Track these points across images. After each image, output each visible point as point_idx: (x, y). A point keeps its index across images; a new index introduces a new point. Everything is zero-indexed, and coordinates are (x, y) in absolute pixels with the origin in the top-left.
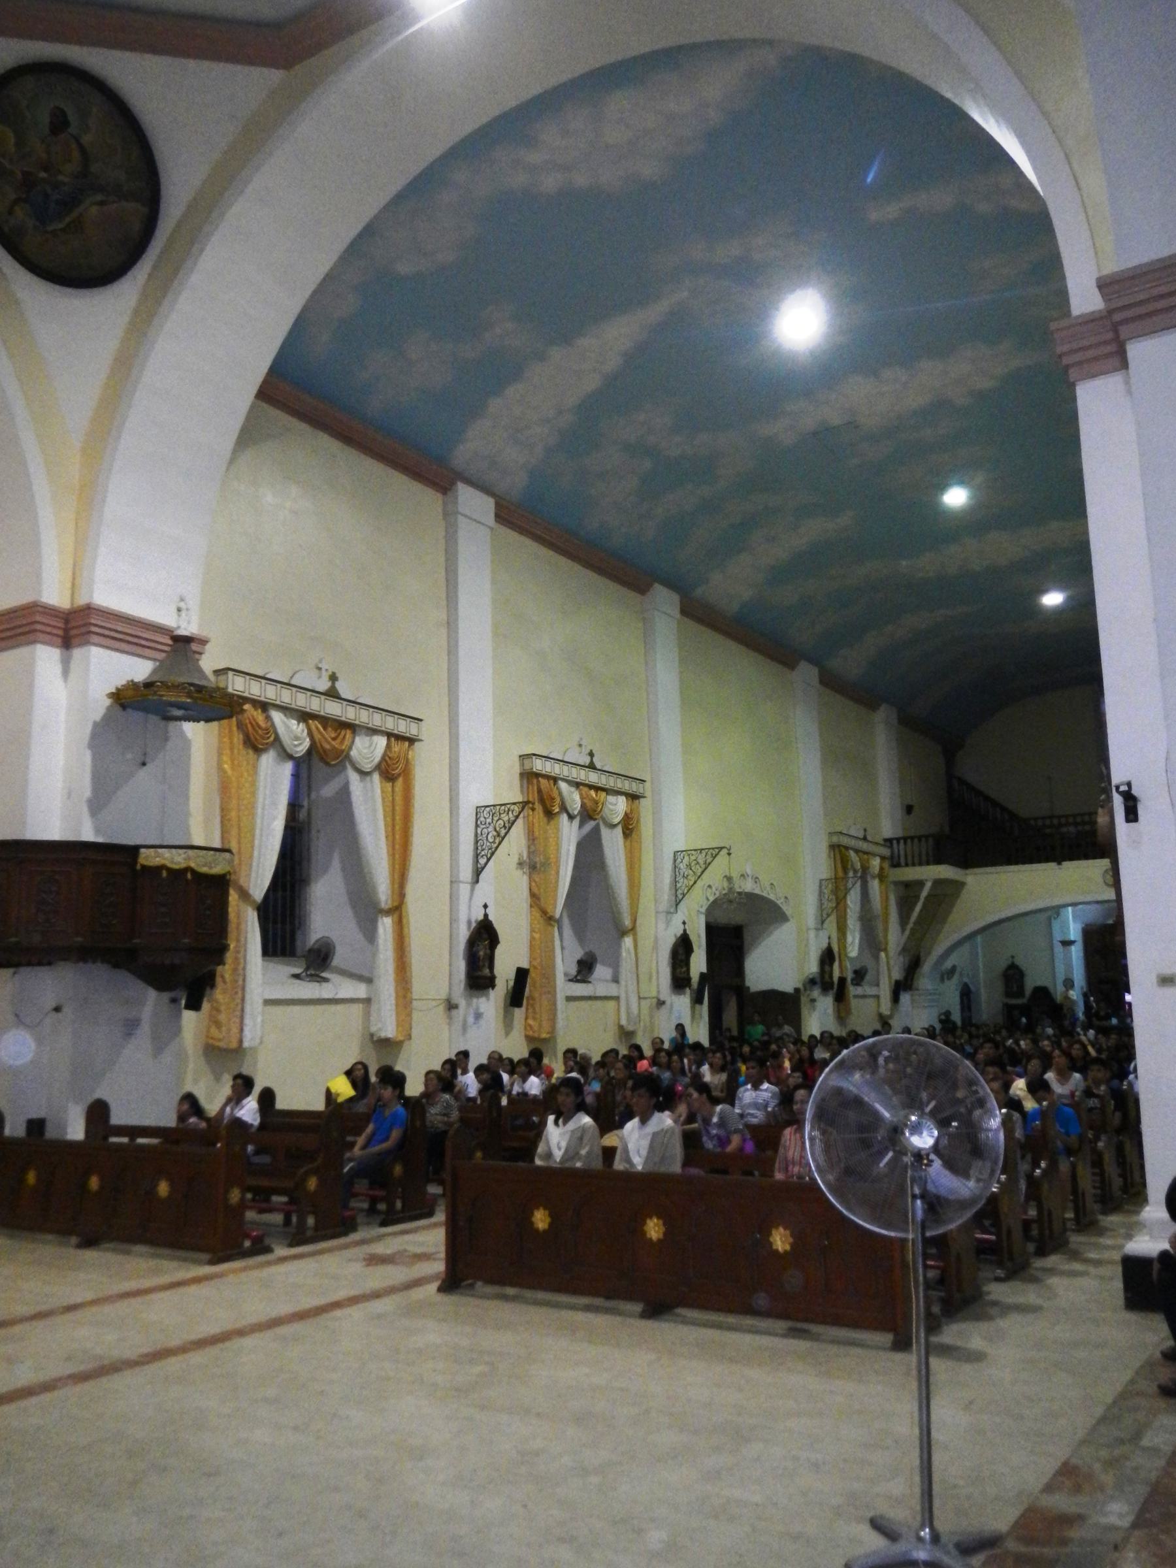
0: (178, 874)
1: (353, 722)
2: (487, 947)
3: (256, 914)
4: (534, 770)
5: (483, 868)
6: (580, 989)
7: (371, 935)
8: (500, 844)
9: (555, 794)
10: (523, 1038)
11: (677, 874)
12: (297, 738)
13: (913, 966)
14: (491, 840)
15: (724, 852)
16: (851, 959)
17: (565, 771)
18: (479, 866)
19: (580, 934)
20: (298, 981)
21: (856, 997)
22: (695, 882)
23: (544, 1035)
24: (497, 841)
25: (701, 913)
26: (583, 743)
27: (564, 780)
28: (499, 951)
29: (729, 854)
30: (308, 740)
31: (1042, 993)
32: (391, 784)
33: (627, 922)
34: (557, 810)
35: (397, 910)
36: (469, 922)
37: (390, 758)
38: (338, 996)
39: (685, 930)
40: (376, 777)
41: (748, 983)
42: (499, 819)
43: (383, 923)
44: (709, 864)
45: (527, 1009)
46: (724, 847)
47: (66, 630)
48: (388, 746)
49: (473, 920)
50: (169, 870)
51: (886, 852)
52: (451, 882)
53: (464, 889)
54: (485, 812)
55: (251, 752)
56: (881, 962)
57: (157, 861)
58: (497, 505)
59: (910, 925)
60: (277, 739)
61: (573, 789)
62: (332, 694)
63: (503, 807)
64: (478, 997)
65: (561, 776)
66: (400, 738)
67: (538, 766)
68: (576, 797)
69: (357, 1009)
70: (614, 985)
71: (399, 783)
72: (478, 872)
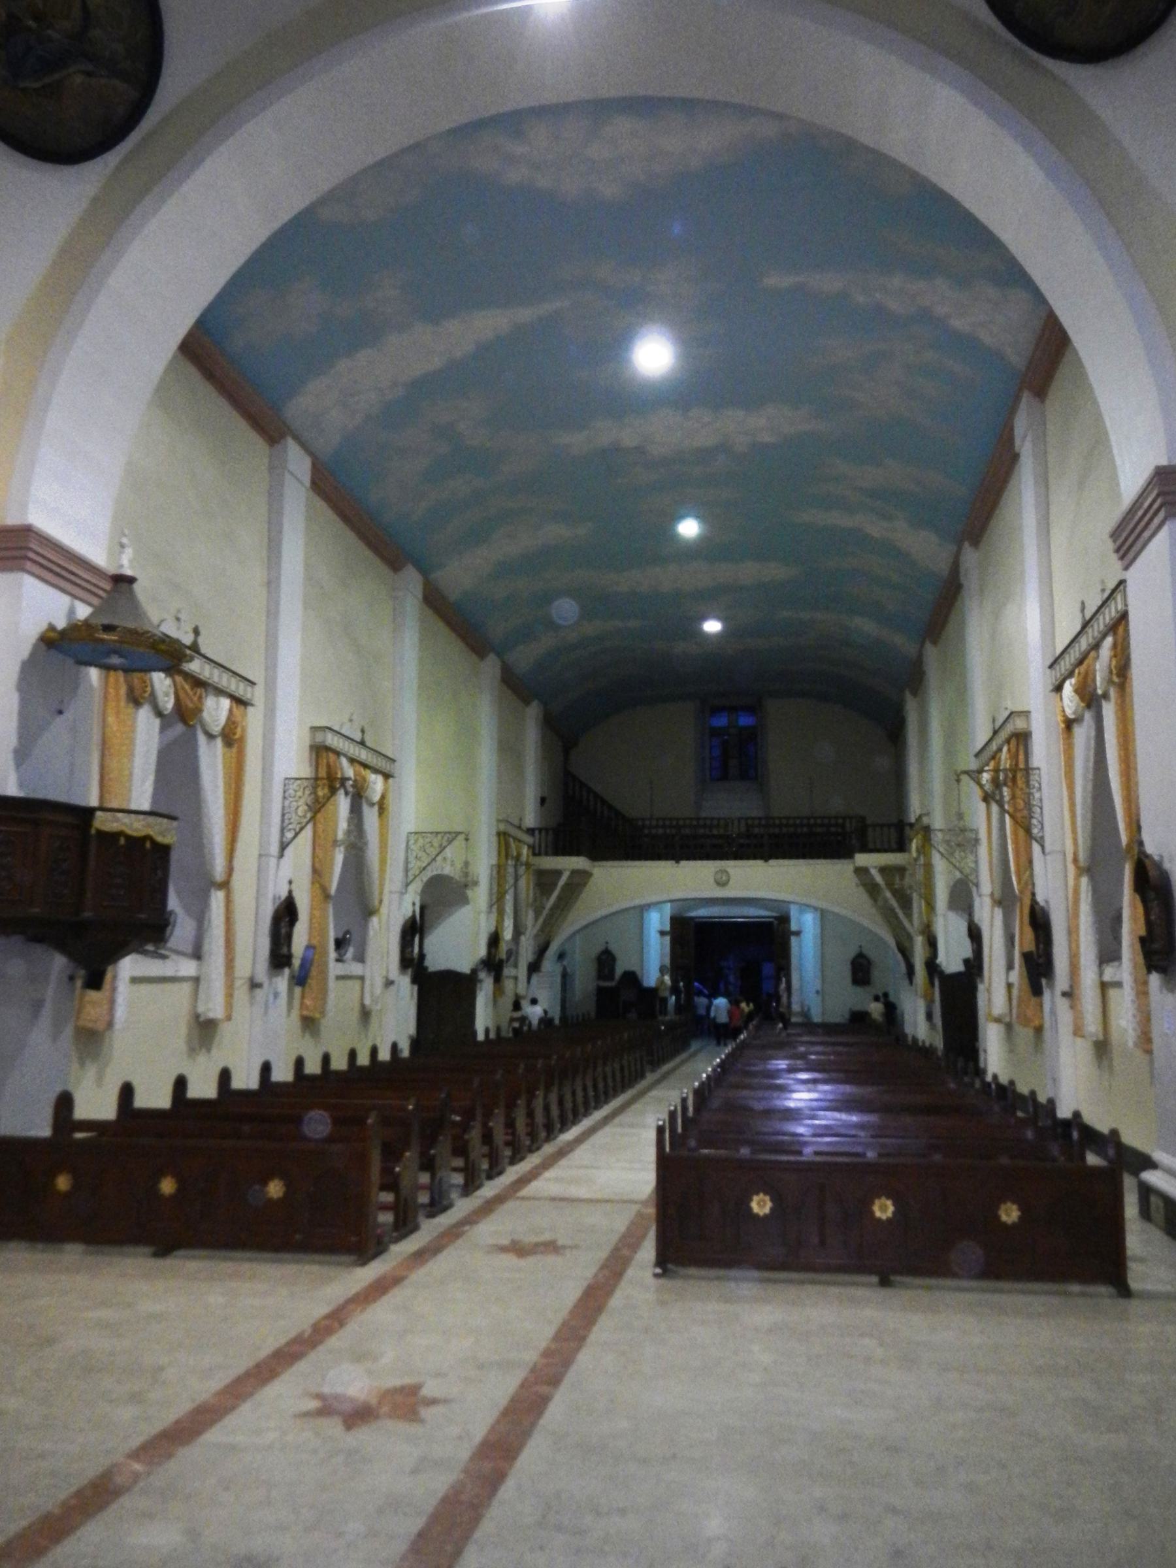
13: (541, 951)
14: (300, 813)
15: (461, 837)
27: (345, 756)
29: (467, 840)
31: (631, 978)
35: (225, 885)
36: (274, 898)
40: (219, 742)
50: (129, 838)
51: (528, 839)
52: (260, 856)
58: (314, 465)
59: (545, 912)
67: (332, 740)
69: (187, 987)
71: (234, 750)
72: (283, 847)
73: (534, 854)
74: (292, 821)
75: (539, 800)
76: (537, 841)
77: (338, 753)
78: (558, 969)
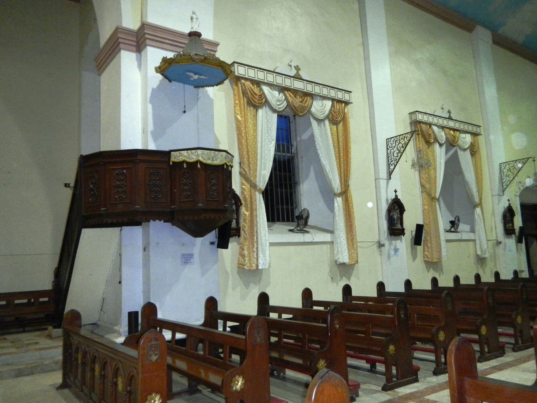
0: (193, 165)
1: (312, 92)
3: (261, 196)
4: (418, 119)
5: (393, 171)
6: (452, 236)
7: (332, 208)
8: (401, 156)
9: (430, 132)
10: (423, 261)
11: (502, 175)
12: (278, 101)
15: (531, 160)
17: (435, 120)
18: (390, 170)
19: (450, 208)
20: (294, 234)
22: (514, 178)
23: (435, 260)
24: (399, 155)
25: (517, 196)
28: (405, 215)
29: (534, 161)
30: (285, 102)
32: (336, 126)
33: (477, 200)
34: (433, 141)
35: (345, 193)
36: (387, 200)
37: (334, 112)
38: (314, 241)
39: (510, 204)
40: (327, 122)
42: (399, 143)
43: (337, 202)
45: (424, 246)
46: (530, 158)
47: (138, 42)
48: (333, 106)
50: (188, 163)
52: (375, 179)
53: (383, 183)
54: (391, 141)
55: (252, 108)
57: (181, 159)
60: (267, 101)
61: (441, 130)
62: (298, 77)
63: (401, 137)
64: (395, 240)
65: (433, 123)
66: (340, 101)
67: (420, 117)
68: (443, 134)
69: (326, 247)
71: (341, 125)
74: (392, 160)
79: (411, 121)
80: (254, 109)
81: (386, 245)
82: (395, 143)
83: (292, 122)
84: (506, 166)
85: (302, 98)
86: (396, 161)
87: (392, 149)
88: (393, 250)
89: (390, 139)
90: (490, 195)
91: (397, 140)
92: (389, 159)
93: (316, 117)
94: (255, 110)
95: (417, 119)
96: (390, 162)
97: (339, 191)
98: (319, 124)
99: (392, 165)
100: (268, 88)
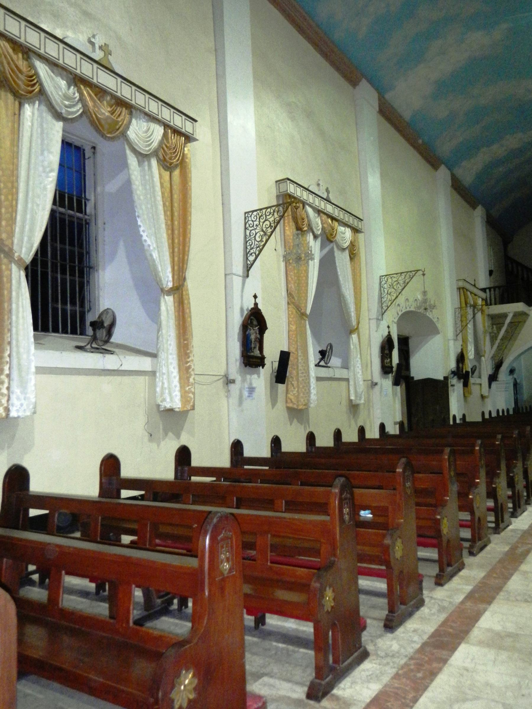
2: (258, 332)
3: (23, 274)
4: (289, 191)
5: (252, 265)
6: (323, 372)
8: (267, 241)
10: (285, 409)
11: (382, 292)
13: (498, 366)
14: (258, 239)
15: (421, 273)
16: (470, 360)
17: (311, 199)
18: (249, 262)
21: (474, 384)
22: (397, 297)
23: (300, 407)
24: (264, 240)
26: (321, 182)
27: (311, 206)
28: (267, 336)
29: (424, 275)
30: (80, 105)
32: (168, 173)
33: (354, 323)
36: (242, 310)
37: (166, 146)
38: (123, 368)
40: (154, 162)
41: (412, 375)
42: (266, 220)
44: (408, 283)
46: (419, 270)
48: (165, 135)
49: (245, 308)
51: (483, 295)
52: (226, 275)
53: (237, 281)
54: (253, 216)
56: (482, 364)
59: (498, 341)
60: (42, 92)
63: (269, 210)
64: (251, 374)
66: (177, 132)
67: (292, 189)
68: (319, 221)
69: (142, 381)
70: (345, 371)
71: (177, 173)
72: (248, 268)
73: (487, 305)
74: (252, 246)
75: (488, 273)
76: (488, 296)
77: (304, 204)
78: (510, 380)
79: (278, 194)
80: (15, 100)
81: (237, 382)
82: (258, 220)
83: (88, 158)
84: (387, 280)
85: (111, 107)
86: (258, 249)
87: (253, 228)
88: (247, 390)
89: (250, 214)
90: (367, 319)
91: (261, 216)
92: (248, 244)
93: (136, 147)
94: (17, 103)
95: (287, 191)
96: (248, 250)
97: (170, 285)
98: (140, 163)
99: (251, 254)
100: (47, 68)
